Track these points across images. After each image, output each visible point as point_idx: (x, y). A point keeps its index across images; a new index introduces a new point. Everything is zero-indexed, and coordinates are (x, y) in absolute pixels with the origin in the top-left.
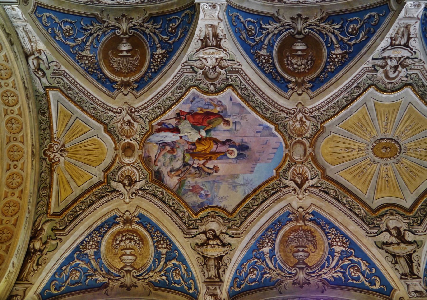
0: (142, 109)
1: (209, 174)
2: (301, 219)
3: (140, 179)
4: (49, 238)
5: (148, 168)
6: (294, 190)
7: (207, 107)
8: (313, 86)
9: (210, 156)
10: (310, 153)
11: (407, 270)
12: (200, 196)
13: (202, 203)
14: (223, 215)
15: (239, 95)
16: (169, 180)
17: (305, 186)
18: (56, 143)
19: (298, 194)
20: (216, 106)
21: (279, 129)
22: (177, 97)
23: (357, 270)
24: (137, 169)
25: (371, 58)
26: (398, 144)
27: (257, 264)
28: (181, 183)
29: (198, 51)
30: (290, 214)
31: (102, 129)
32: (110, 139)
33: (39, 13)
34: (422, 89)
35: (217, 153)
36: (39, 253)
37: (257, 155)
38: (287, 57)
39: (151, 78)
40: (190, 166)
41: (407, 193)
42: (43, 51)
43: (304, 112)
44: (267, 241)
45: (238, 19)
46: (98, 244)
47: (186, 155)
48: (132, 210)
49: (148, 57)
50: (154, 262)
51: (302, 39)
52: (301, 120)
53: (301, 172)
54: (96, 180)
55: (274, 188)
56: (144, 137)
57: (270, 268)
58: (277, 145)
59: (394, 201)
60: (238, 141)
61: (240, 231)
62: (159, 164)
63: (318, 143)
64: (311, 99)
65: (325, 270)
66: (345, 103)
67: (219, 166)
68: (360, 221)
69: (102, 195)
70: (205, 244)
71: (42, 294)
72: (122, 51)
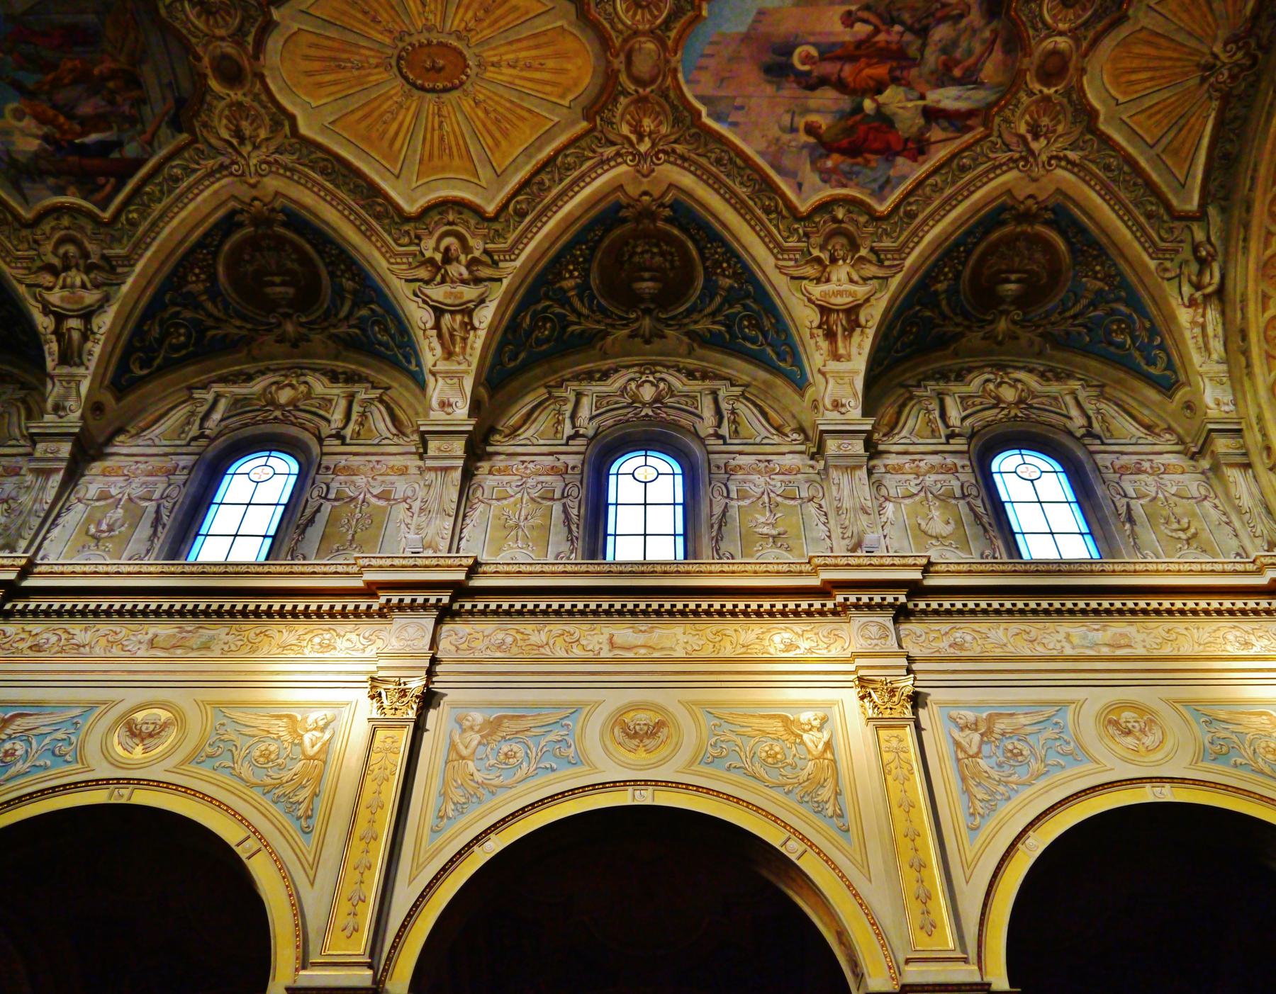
0: (1000, 166)
7: (856, 168)
8: (617, 212)
10: (617, 56)
15: (783, 196)
18: (1218, 86)
20: (834, 170)
21: (691, 114)
22: (920, 192)
25: (505, 282)
26: (406, 78)
29: (867, 300)
31: (1102, 118)
32: (1089, 95)
33: (1169, 378)
34: (378, 208)
38: (673, 268)
39: (969, 233)
40: (910, 29)
42: (1184, 304)
43: (634, 156)
45: (778, 354)
49: (967, 273)
51: (642, 300)
52: (641, 138)
53: (640, 12)
60: (788, 85)
62: (987, 34)
63: (600, 81)
64: (621, 186)
66: (545, 177)
67: (838, 27)
72: (1018, 281)
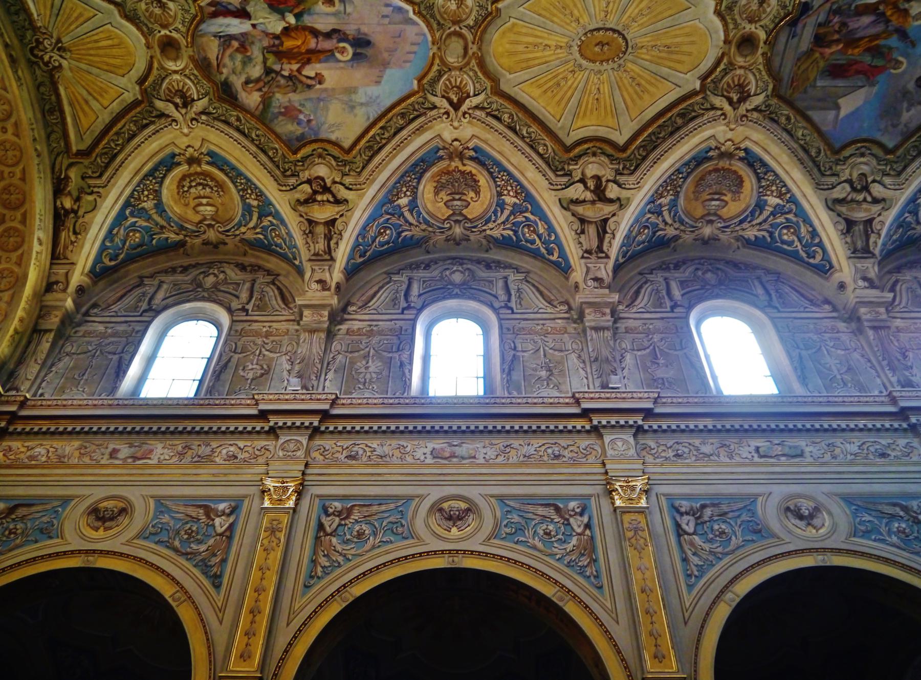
1: (309, 87)
2: (457, 156)
3: (198, 95)
4: (81, 191)
5: (209, 78)
6: (447, 113)
9: (307, 56)
10: (474, 54)
11: (595, 243)
12: (298, 124)
13: (303, 134)
14: (336, 152)
16: (247, 98)
17: (464, 108)
18: (46, 36)
19: (452, 120)
23: (532, 231)
24: (190, 79)
26: (624, 38)
27: (390, 221)
28: (266, 102)
30: (439, 149)
35: (319, 51)
36: (72, 215)
37: (386, 55)
40: (277, 73)
41: (624, 119)
44: (404, 189)
46: (157, 194)
47: (267, 55)
48: (197, 145)
50: (243, 215)
54: (129, 97)
55: (414, 110)
56: (190, 26)
57: (411, 224)
58: (420, 39)
59: (602, 132)
60: (353, 32)
61: (362, 179)
62: (225, 71)
63: (487, 36)
65: (490, 225)
67: (325, 73)
68: (544, 166)
69: (145, 122)
70: (309, 200)
71: (92, 271)
